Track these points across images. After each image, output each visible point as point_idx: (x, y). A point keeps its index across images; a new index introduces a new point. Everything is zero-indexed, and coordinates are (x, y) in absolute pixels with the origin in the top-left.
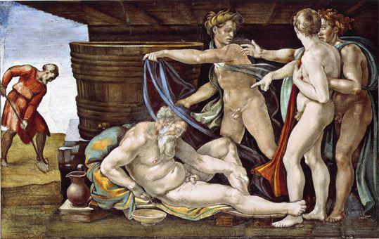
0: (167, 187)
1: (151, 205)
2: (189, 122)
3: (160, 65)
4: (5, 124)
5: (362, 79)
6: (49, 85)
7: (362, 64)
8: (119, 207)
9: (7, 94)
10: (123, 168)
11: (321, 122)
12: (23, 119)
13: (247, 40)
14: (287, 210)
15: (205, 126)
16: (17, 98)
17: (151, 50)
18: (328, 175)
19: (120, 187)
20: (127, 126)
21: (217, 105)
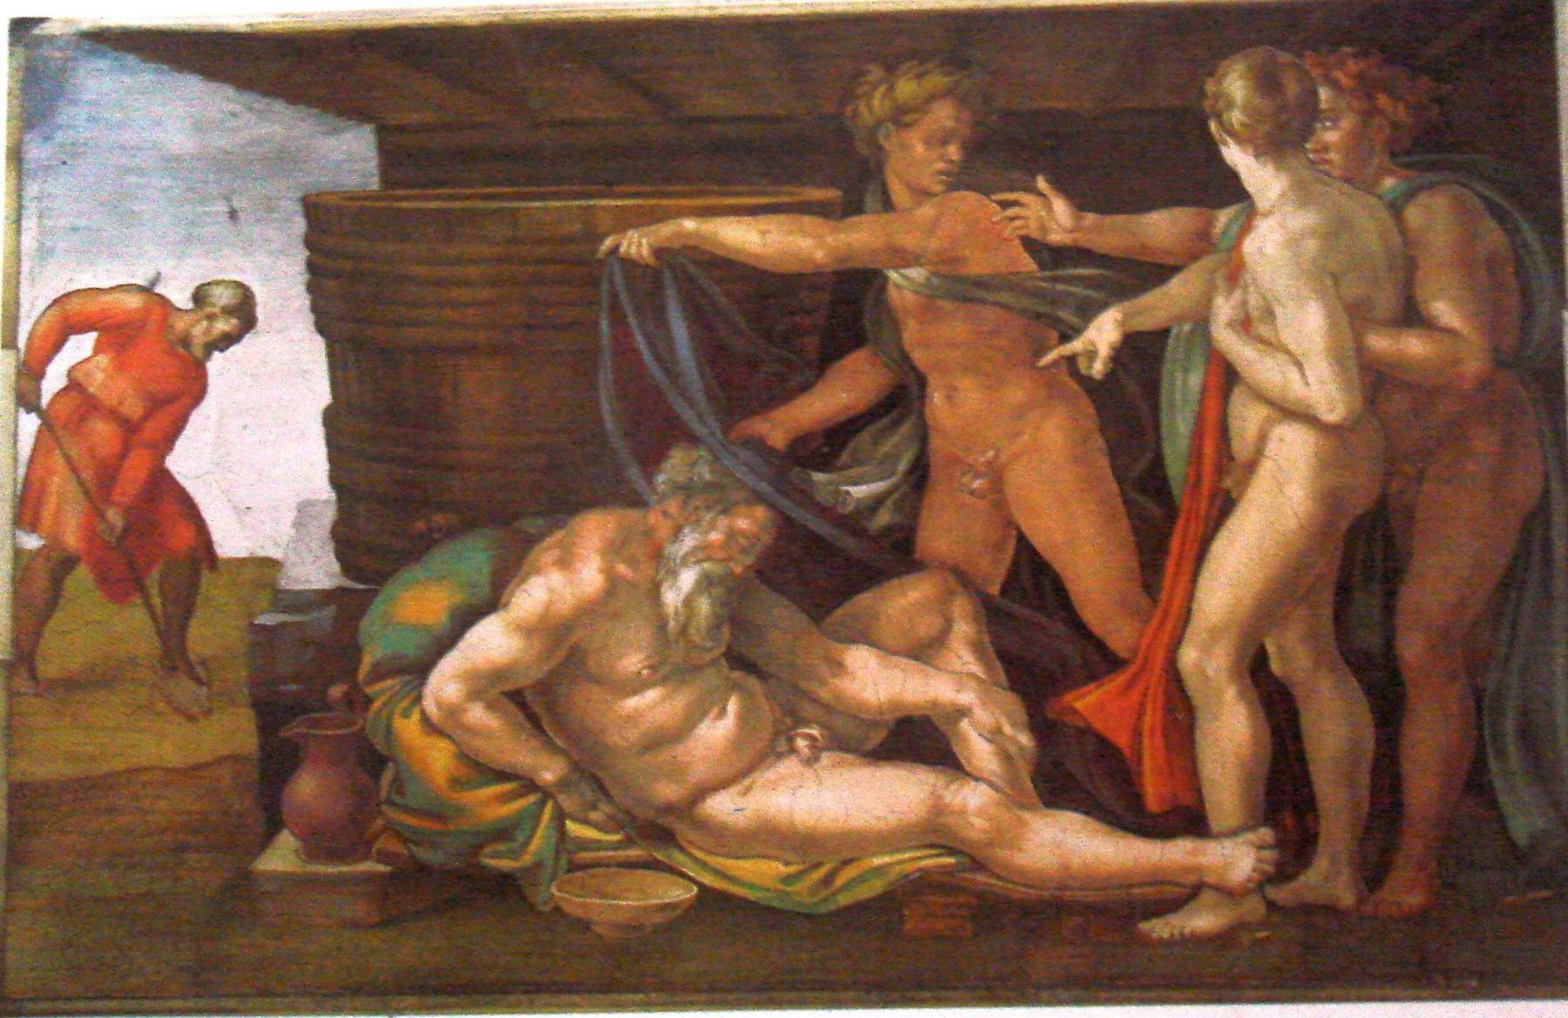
0: (700, 772)
1: (634, 853)
2: (784, 503)
3: (667, 274)
4: (33, 527)
5: (1491, 320)
6: (217, 364)
7: (1491, 262)
8: (498, 861)
9: (45, 400)
10: (517, 697)
11: (1330, 501)
12: (108, 501)
13: (1015, 175)
14: (1197, 869)
15: (853, 522)
16: (83, 419)
17: (626, 221)
18: (1365, 718)
19: (502, 776)
20: (531, 525)
21: (897, 444)
